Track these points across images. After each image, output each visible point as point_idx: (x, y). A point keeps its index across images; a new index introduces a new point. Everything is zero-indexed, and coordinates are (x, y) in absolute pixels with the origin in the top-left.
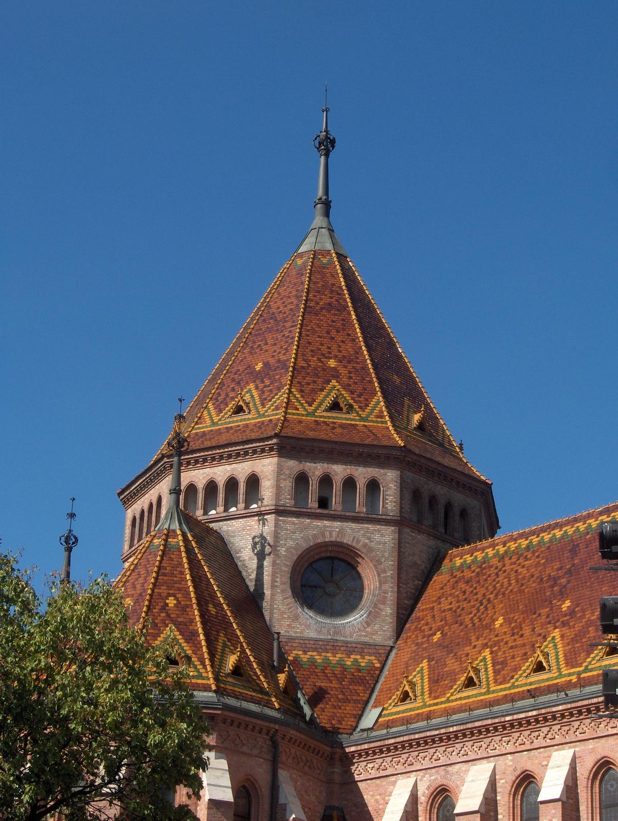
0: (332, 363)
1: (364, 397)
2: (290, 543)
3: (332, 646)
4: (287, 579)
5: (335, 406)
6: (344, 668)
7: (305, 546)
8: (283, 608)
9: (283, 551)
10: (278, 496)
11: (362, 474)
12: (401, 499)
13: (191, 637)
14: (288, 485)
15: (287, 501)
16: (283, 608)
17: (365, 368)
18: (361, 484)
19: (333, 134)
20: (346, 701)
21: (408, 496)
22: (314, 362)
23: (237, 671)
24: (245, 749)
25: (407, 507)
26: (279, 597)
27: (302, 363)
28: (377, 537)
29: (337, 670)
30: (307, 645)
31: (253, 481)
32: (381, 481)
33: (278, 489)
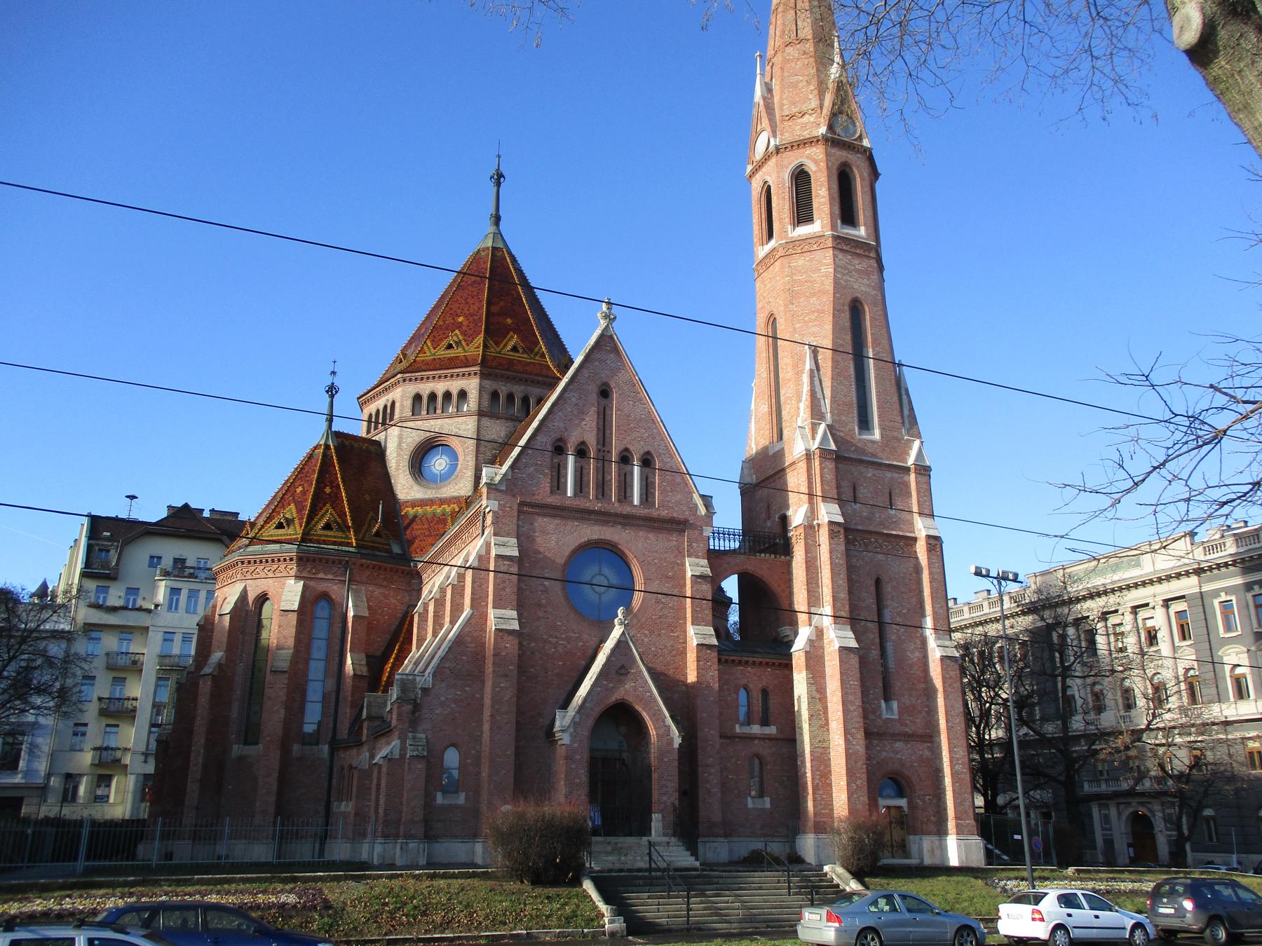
0: (460, 319)
1: (469, 338)
2: (409, 440)
3: (431, 502)
5: (450, 347)
6: (434, 515)
9: (404, 446)
12: (480, 398)
14: (409, 403)
17: (480, 319)
18: (455, 393)
19: (503, 170)
21: (486, 396)
22: (449, 320)
23: (328, 527)
24: (321, 575)
25: (486, 403)
26: (401, 476)
27: (441, 323)
28: (463, 427)
29: (429, 516)
30: (414, 504)
32: (467, 389)
33: (402, 406)
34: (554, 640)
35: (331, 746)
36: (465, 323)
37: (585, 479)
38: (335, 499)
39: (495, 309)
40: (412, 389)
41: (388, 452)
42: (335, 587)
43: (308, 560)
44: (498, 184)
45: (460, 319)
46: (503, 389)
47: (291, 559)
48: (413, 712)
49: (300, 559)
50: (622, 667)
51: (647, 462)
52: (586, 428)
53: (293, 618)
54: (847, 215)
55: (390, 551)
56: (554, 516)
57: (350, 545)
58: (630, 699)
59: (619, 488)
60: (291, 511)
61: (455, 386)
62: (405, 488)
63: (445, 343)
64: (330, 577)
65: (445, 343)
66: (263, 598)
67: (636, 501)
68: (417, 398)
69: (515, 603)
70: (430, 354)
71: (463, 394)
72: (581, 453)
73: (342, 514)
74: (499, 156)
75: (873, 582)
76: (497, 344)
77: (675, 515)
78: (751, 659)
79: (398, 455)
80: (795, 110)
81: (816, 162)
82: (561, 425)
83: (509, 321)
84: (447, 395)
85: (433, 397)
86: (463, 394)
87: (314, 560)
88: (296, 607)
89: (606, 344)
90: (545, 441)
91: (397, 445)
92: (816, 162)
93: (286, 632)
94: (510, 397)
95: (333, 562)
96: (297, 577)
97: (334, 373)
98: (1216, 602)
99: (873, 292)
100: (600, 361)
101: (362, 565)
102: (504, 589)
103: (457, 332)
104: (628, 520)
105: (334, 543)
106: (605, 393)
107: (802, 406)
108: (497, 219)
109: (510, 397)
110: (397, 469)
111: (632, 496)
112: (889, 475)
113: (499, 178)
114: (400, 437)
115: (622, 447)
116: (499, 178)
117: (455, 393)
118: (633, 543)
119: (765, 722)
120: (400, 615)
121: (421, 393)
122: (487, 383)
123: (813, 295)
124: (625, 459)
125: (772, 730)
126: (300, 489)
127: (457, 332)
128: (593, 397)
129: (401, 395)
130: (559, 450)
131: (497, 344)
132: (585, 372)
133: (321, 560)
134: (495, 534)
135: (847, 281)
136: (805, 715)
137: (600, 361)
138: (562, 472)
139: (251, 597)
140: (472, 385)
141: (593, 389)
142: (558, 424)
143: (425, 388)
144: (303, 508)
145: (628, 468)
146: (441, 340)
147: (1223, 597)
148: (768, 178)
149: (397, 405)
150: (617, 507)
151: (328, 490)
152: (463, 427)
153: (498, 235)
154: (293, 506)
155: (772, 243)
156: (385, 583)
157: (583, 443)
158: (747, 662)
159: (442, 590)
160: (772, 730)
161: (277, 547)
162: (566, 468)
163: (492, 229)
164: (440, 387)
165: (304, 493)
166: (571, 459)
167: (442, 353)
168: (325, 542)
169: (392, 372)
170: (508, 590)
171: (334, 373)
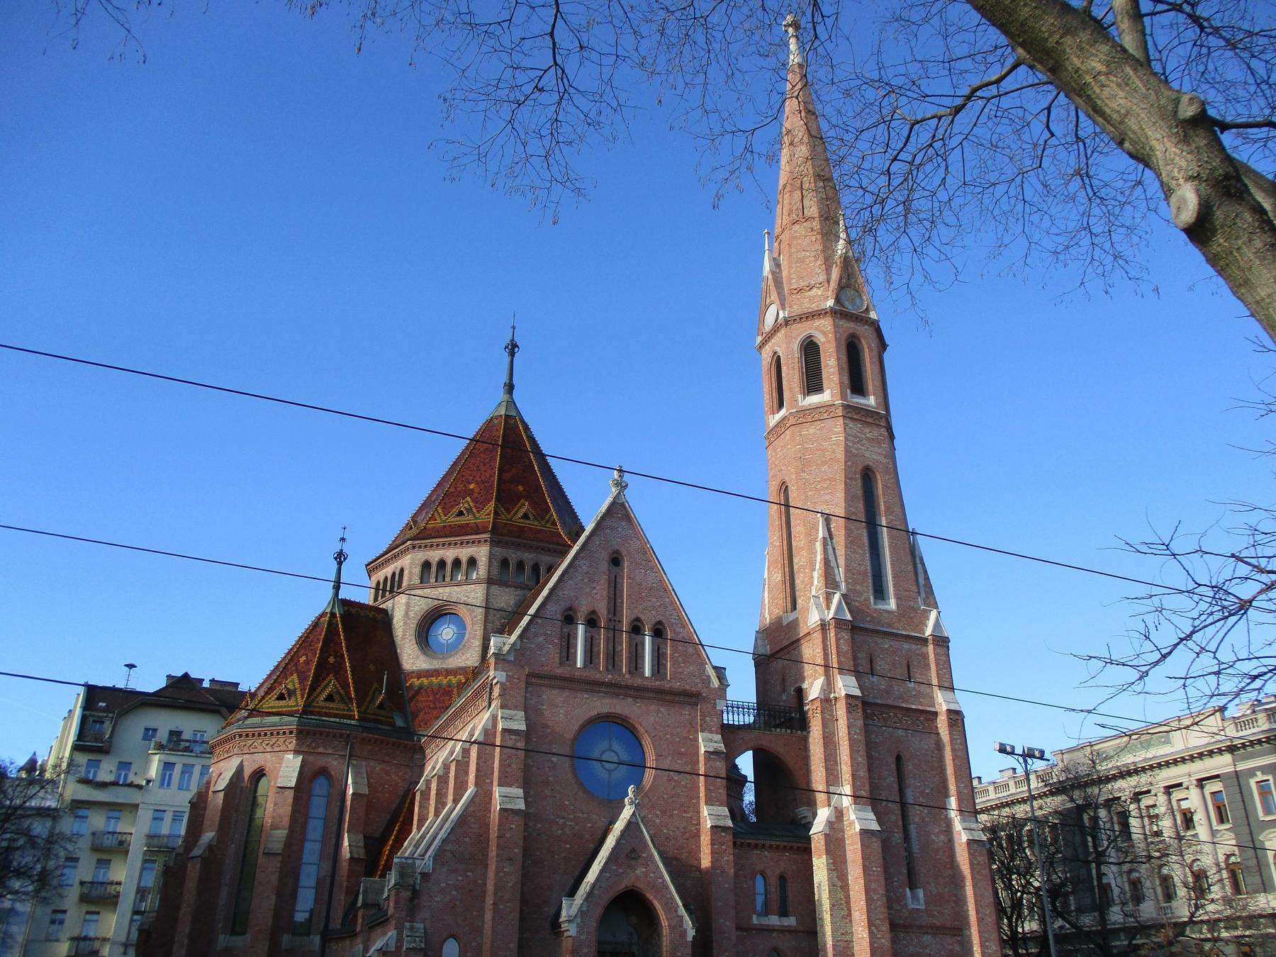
0: (472, 486)
1: (480, 504)
3: (437, 673)
4: (413, 632)
5: (461, 513)
6: (440, 685)
7: (426, 608)
8: (410, 652)
9: (411, 614)
10: (410, 579)
11: (464, 553)
13: (302, 680)
14: (417, 570)
15: (416, 581)
16: (410, 652)
17: (492, 486)
18: (464, 560)
20: (435, 708)
21: (496, 564)
22: (461, 487)
23: (330, 698)
24: (321, 750)
25: (495, 571)
26: (407, 645)
28: (472, 595)
29: (435, 688)
30: (420, 674)
31: (402, 570)
32: (476, 556)
33: (410, 573)
34: (562, 821)
35: (322, 937)
36: (477, 490)
37: (595, 649)
38: (338, 669)
39: (507, 476)
40: (421, 556)
41: (395, 621)
42: (335, 763)
43: (308, 733)
44: (512, 354)
45: (472, 486)
46: (514, 556)
47: (291, 733)
48: (411, 900)
49: (300, 732)
50: (633, 850)
51: (658, 632)
52: (598, 596)
53: (290, 795)
54: (856, 384)
55: (392, 724)
56: (563, 688)
57: (351, 717)
58: (641, 885)
59: (629, 659)
60: (293, 681)
61: (464, 553)
62: (411, 658)
63: (456, 510)
64: (330, 751)
65: (456, 510)
66: (259, 774)
67: (647, 673)
68: (426, 565)
69: (521, 780)
70: (441, 520)
71: (472, 562)
72: (592, 622)
73: (345, 686)
74: (514, 328)
75: (893, 760)
76: (508, 511)
77: (687, 687)
78: (767, 843)
79: (405, 624)
80: (803, 284)
81: (825, 334)
82: (572, 594)
83: (520, 488)
84: (457, 563)
85: (442, 564)
86: (472, 562)
87: (314, 734)
88: (293, 784)
89: (618, 512)
90: (555, 610)
91: (404, 612)
92: (825, 333)
93: (281, 811)
94: (520, 565)
95: (334, 736)
96: (296, 752)
97: (343, 539)
98: (1252, 782)
99: (885, 461)
100: (612, 528)
101: (363, 739)
102: (509, 766)
103: (468, 499)
104: (640, 692)
105: (336, 716)
106: (616, 561)
107: (816, 574)
108: (510, 388)
109: (520, 565)
110: (404, 638)
111: (643, 668)
112: (906, 646)
113: (513, 348)
114: (408, 605)
115: (633, 617)
116: (513, 348)
117: (464, 560)
118: (645, 716)
119: (783, 913)
120: (401, 793)
121: (431, 560)
122: (497, 550)
123: (825, 463)
124: (636, 629)
125: (791, 921)
126: (304, 658)
127: (468, 499)
128: (604, 565)
129: (410, 562)
130: (569, 619)
131: (508, 511)
132: (596, 540)
133: (321, 733)
134: (502, 707)
135: (857, 449)
136: (829, 943)
137: (612, 528)
138: (572, 641)
139: (247, 772)
140: (482, 553)
141: (604, 557)
142: (567, 592)
143: (434, 555)
144: (306, 678)
145: (639, 638)
146: (452, 507)
147: (1260, 777)
148: (777, 349)
149: (406, 572)
150: (628, 679)
151: (332, 660)
152: (472, 595)
153: (511, 403)
154: (295, 676)
155: (783, 412)
156: (387, 758)
157: (594, 612)
158: (763, 846)
159: (446, 766)
160: (791, 921)
161: (276, 719)
162: (576, 638)
163: (506, 397)
164: (450, 554)
165: (307, 662)
166: (581, 629)
167: (453, 520)
168: (326, 715)
169: (402, 539)
170: (514, 766)
171: (343, 539)
